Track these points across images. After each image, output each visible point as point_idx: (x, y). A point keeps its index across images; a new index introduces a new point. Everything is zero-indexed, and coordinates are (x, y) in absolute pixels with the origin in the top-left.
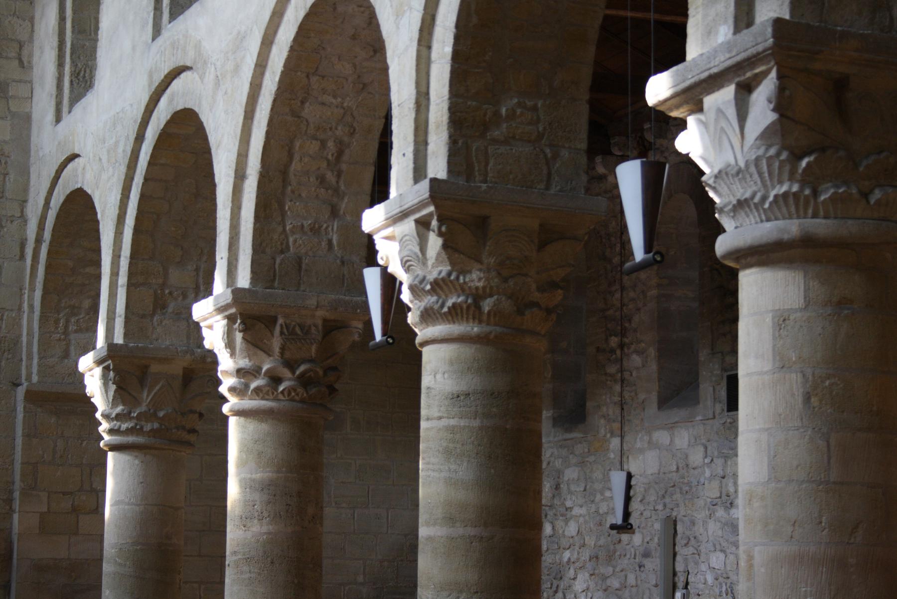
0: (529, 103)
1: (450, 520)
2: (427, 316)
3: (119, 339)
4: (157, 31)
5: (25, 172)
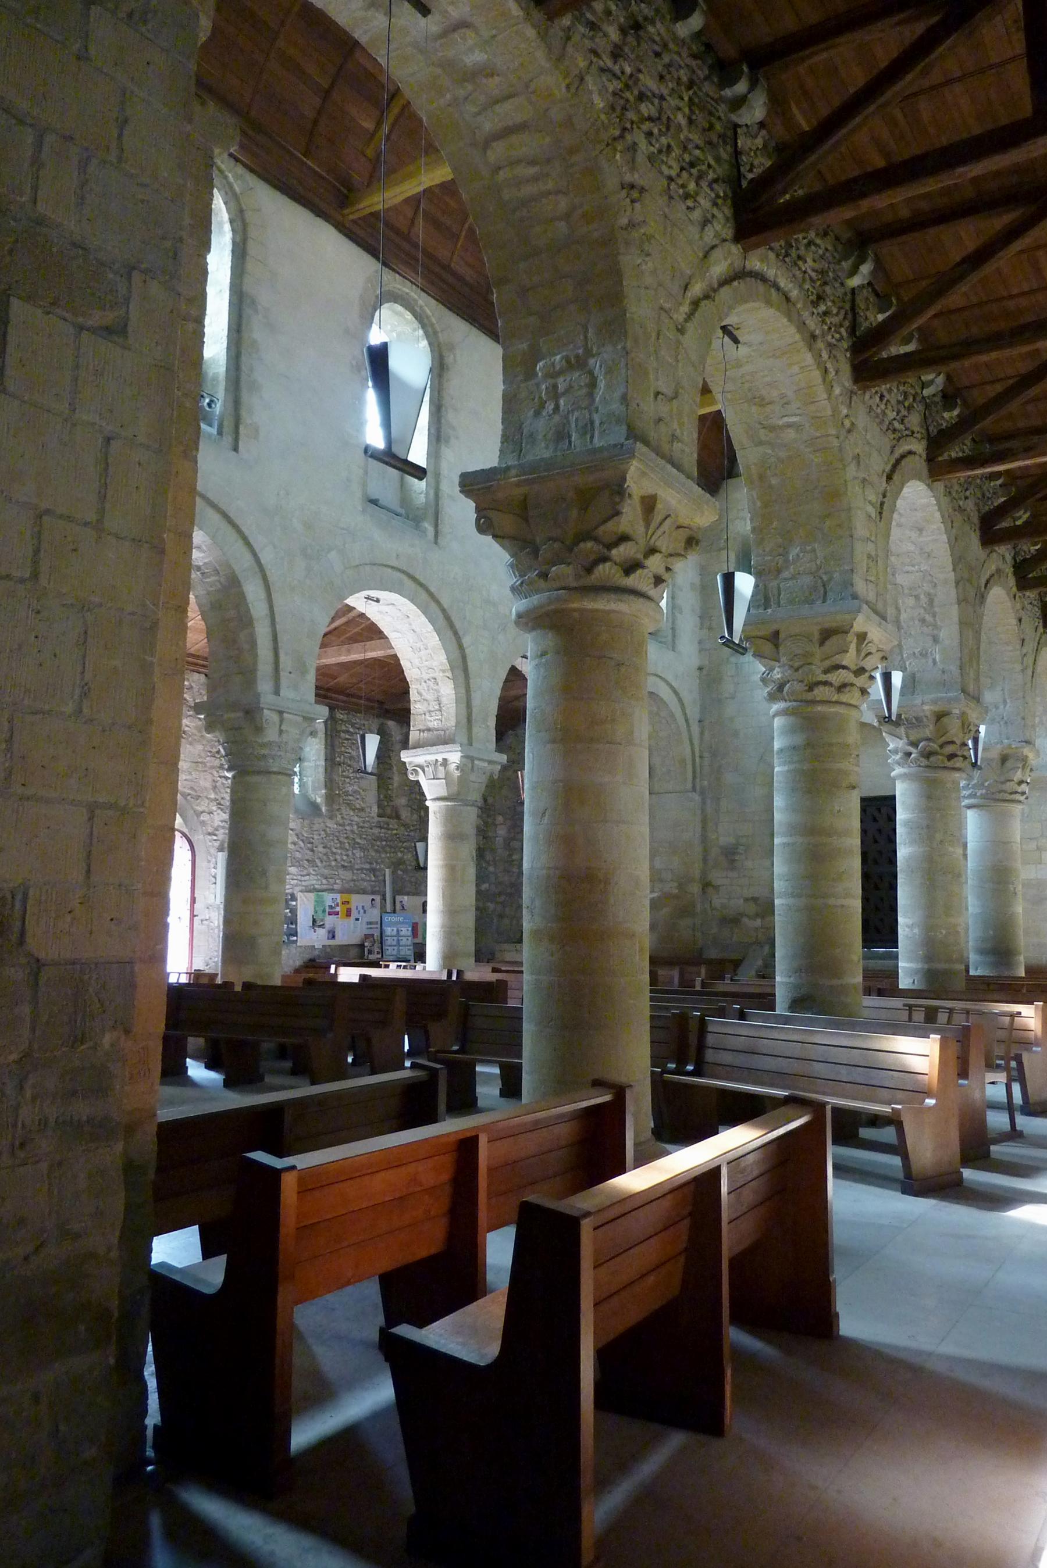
0: (809, 548)
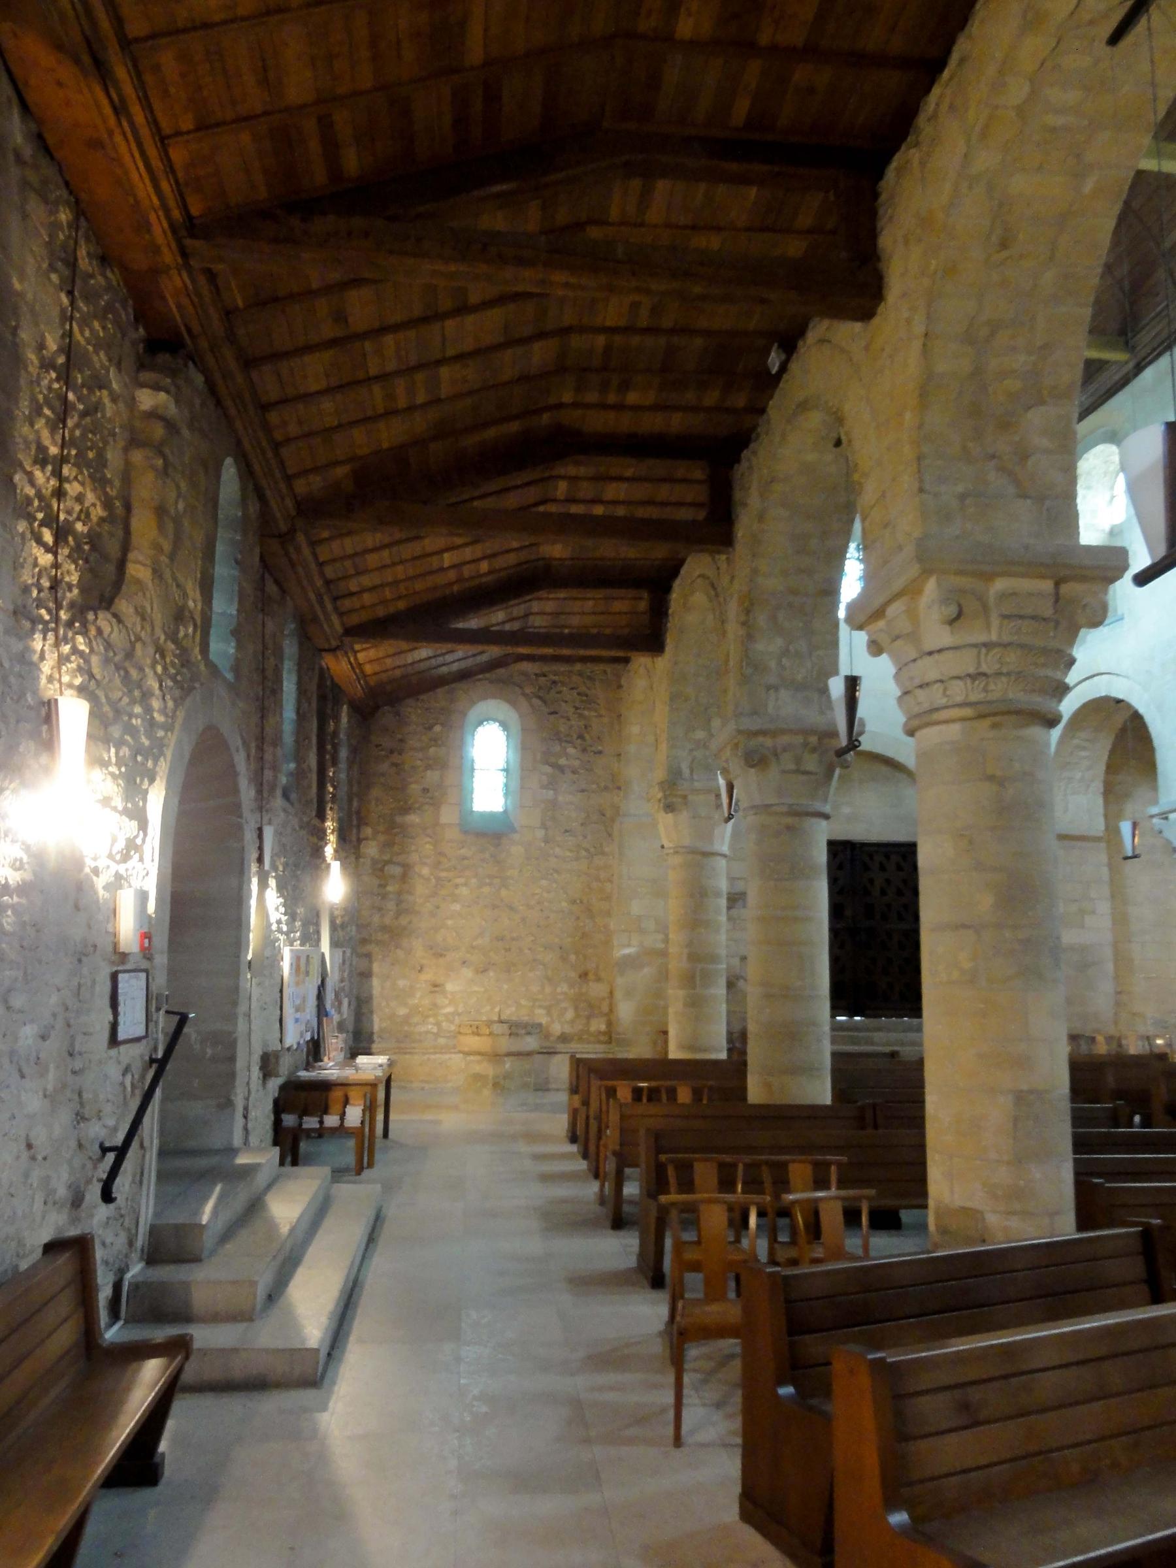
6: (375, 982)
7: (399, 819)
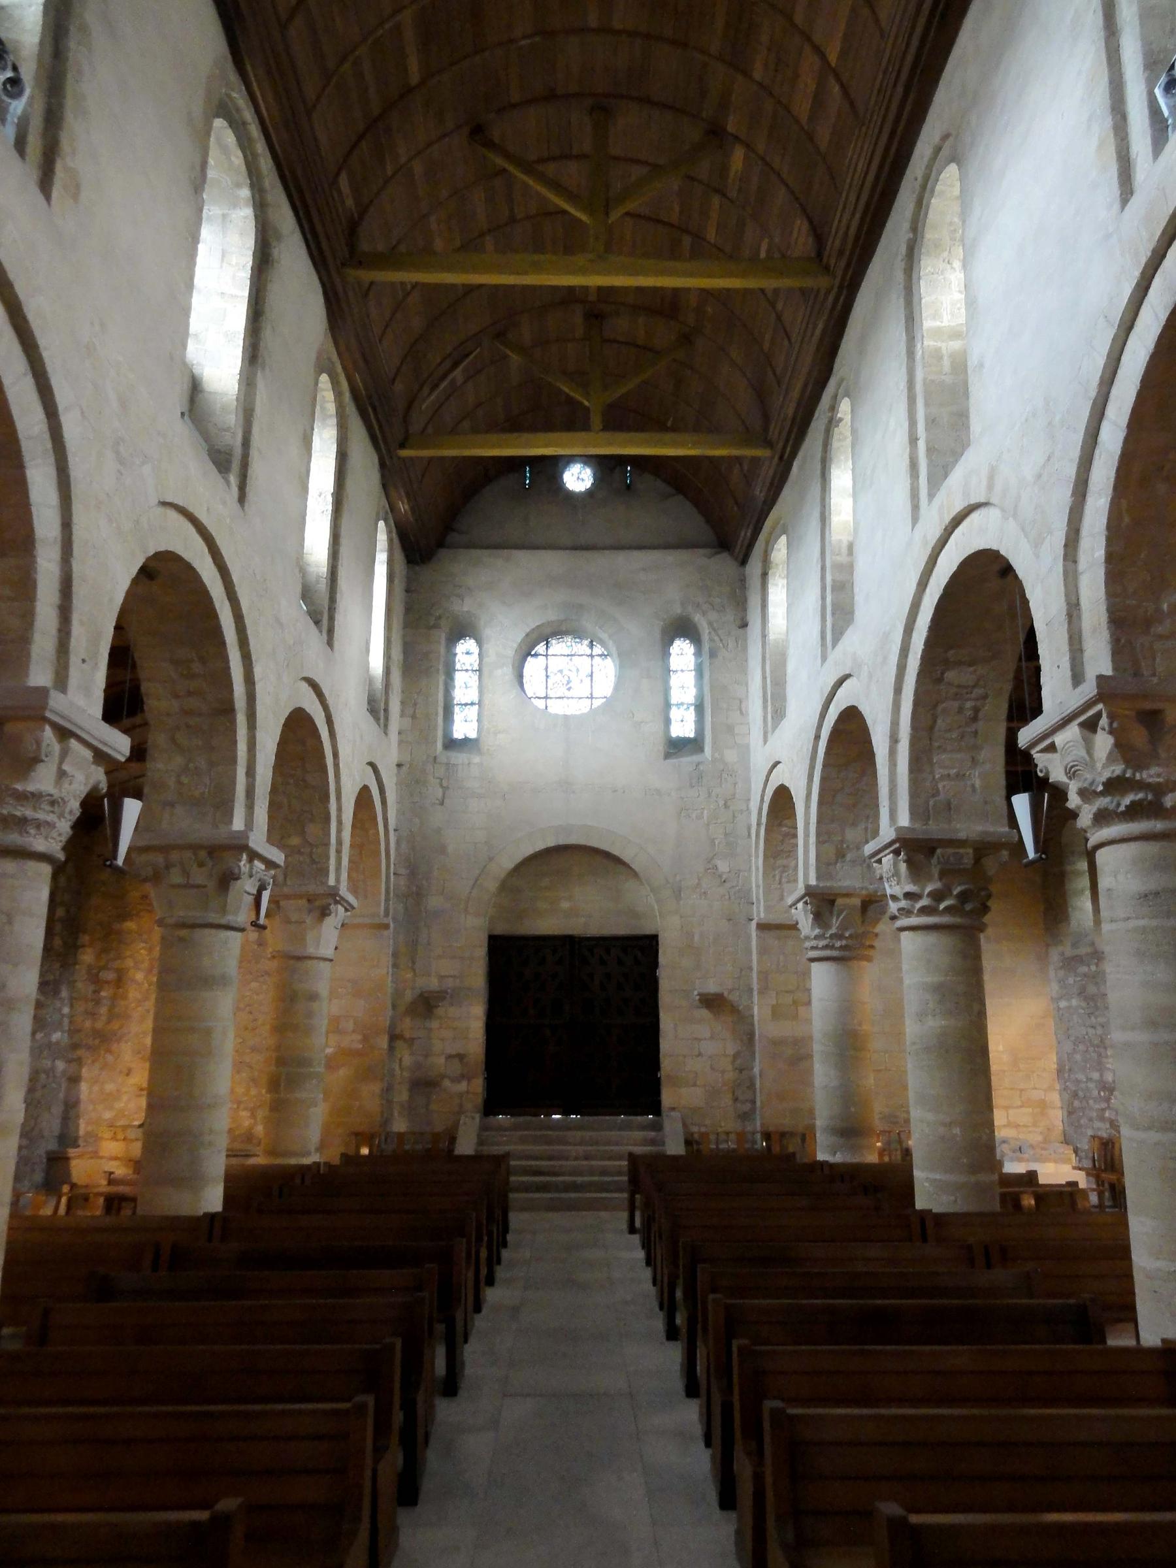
1: (1152, 1024)
2: (1102, 817)
3: (813, 881)
4: (824, 658)
5: (748, 781)
6: (84, 1087)
7: (116, 926)
